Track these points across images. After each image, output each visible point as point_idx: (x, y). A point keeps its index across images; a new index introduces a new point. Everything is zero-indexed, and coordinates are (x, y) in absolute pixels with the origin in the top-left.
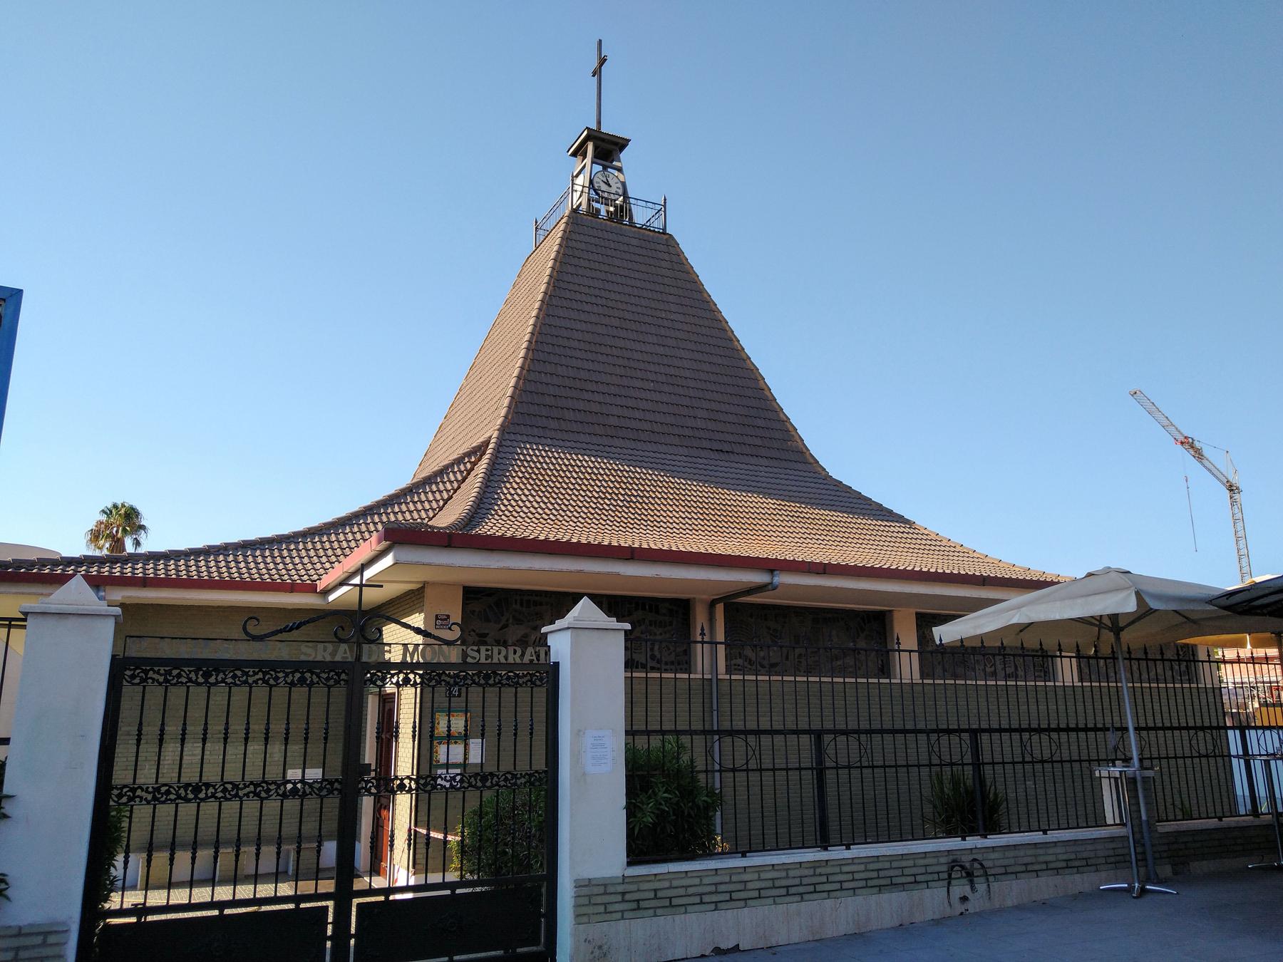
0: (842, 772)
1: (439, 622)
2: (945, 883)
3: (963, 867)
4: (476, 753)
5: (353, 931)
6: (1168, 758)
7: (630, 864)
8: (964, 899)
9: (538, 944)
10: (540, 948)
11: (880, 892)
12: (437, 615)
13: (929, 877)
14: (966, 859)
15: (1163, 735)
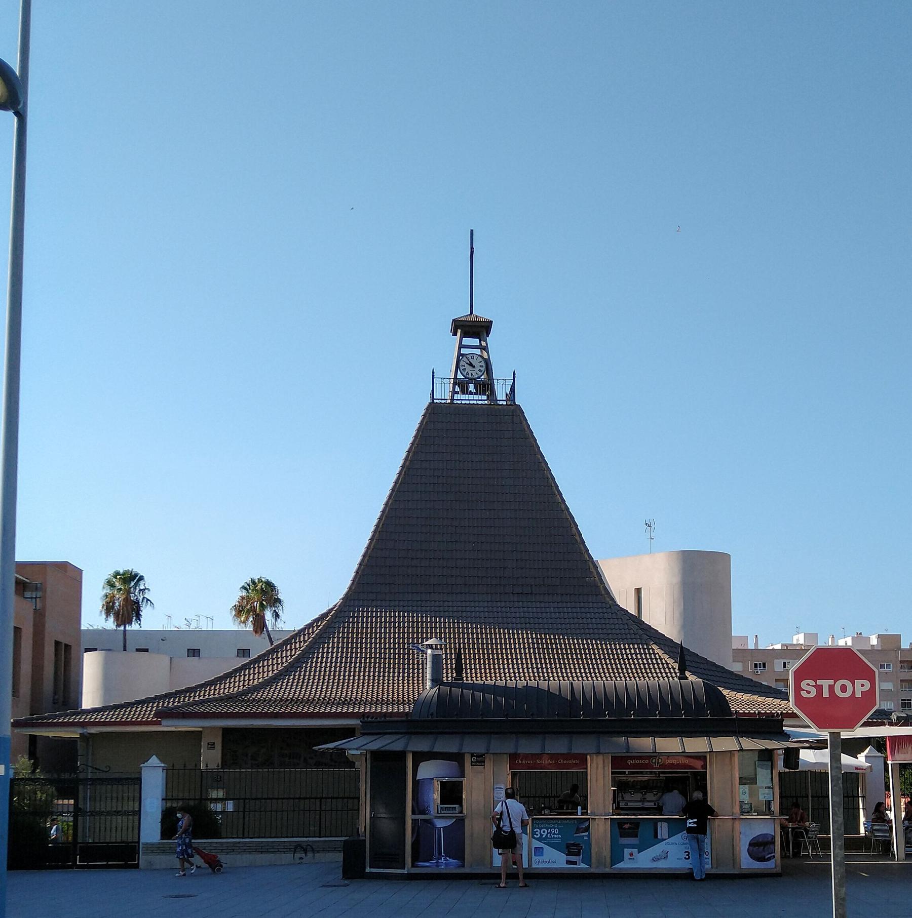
0: (279, 813)
1: (210, 746)
2: (293, 852)
3: (302, 847)
4: (230, 806)
5: (105, 863)
6: (304, 810)
7: (161, 839)
8: (301, 858)
9: (135, 861)
10: (136, 862)
11: (262, 854)
12: (208, 743)
13: (285, 850)
14: (304, 845)
15: (129, 807)
